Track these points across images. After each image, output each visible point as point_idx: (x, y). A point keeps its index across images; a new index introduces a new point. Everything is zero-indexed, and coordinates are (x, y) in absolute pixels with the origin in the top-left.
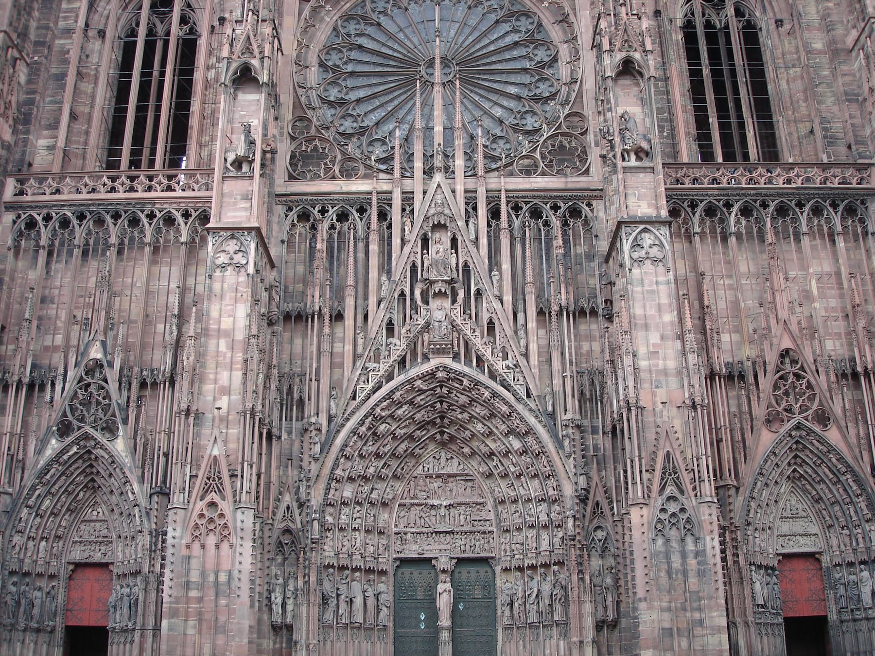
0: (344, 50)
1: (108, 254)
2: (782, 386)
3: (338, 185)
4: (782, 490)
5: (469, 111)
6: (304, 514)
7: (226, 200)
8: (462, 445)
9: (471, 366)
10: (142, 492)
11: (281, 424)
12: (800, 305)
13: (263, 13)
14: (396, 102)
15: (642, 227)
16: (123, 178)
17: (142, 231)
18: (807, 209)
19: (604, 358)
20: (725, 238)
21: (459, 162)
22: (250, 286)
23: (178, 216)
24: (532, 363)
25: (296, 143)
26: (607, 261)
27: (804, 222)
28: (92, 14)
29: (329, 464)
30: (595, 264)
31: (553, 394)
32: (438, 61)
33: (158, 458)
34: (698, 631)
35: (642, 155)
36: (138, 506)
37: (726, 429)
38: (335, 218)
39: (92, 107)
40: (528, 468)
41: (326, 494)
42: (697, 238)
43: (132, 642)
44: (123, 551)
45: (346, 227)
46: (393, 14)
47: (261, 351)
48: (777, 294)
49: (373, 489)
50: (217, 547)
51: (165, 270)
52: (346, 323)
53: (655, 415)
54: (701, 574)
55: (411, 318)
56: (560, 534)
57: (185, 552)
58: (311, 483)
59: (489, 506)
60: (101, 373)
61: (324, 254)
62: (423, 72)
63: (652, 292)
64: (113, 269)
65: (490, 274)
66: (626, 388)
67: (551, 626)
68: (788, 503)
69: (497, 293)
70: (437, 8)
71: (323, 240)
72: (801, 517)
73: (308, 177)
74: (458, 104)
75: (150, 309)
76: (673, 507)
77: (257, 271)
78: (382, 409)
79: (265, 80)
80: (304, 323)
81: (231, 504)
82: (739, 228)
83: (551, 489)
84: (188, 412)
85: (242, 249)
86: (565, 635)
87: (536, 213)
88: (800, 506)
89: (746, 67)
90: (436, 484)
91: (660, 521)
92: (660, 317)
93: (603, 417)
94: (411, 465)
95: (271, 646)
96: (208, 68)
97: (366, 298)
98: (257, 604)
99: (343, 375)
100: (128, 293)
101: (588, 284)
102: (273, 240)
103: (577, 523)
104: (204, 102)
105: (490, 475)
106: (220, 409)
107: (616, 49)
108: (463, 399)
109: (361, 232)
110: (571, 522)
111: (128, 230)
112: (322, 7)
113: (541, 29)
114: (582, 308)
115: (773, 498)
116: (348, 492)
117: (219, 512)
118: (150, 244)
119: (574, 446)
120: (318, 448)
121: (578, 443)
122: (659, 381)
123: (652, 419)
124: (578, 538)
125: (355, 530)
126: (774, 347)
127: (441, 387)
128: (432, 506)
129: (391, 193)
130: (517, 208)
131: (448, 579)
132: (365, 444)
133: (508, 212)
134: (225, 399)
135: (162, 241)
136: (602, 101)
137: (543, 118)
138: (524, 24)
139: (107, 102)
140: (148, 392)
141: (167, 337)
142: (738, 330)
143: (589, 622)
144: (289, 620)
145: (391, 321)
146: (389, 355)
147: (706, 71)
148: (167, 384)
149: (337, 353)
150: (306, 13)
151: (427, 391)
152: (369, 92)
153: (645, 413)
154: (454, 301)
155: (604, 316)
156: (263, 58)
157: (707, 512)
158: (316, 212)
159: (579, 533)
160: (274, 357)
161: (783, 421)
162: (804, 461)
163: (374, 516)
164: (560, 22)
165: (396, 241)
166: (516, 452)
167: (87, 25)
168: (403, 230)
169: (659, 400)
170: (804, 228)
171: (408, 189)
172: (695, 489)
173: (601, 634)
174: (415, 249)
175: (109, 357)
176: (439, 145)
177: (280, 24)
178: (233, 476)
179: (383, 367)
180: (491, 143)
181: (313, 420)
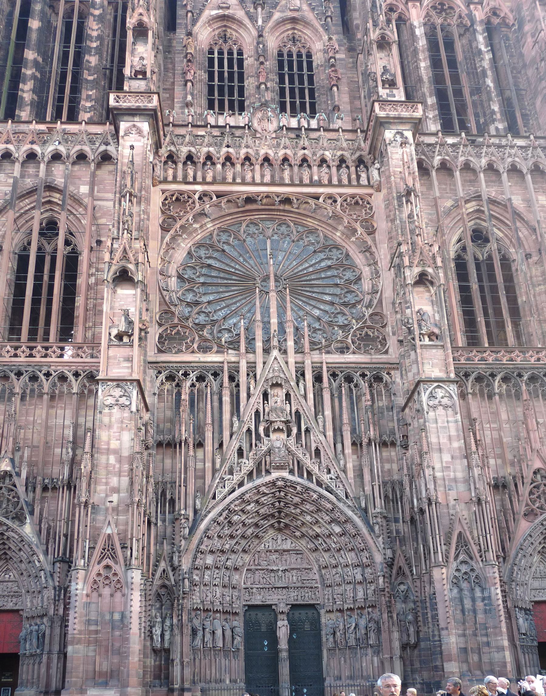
0: (197, 268)
1: (13, 399)
2: (536, 492)
6: (177, 575)
7: (110, 361)
11: (157, 516)
14: (238, 304)
16: (24, 348)
17: (41, 386)
24: (349, 476)
29: (195, 540)
31: (366, 497)
33: (60, 538)
36: (43, 570)
38: (195, 379)
43: (40, 663)
44: (32, 602)
51: (60, 412)
52: (206, 448)
55: (256, 445)
56: (373, 588)
60: (11, 480)
65: (316, 417)
69: (322, 430)
73: (174, 352)
75: (49, 439)
86: (378, 651)
87: (349, 379)
93: (403, 512)
96: (89, 276)
97: (221, 432)
98: (143, 635)
99: (204, 484)
100: (31, 427)
103: (386, 580)
108: (297, 500)
110: (381, 580)
116: (209, 560)
118: (47, 394)
120: (187, 531)
121: (385, 528)
124: (387, 590)
127: (280, 491)
129: (238, 363)
130: (334, 375)
132: (222, 529)
135: (57, 392)
140: (49, 494)
144: (166, 645)
145: (240, 448)
146: (241, 470)
147: (475, 286)
148: (65, 487)
149: (199, 469)
151: (268, 494)
152: (216, 296)
159: (388, 587)
164: (365, 251)
165: (243, 395)
168: (249, 388)
171: (252, 360)
173: (405, 652)
175: (17, 469)
176: (275, 331)
179: (236, 478)
181: (183, 512)
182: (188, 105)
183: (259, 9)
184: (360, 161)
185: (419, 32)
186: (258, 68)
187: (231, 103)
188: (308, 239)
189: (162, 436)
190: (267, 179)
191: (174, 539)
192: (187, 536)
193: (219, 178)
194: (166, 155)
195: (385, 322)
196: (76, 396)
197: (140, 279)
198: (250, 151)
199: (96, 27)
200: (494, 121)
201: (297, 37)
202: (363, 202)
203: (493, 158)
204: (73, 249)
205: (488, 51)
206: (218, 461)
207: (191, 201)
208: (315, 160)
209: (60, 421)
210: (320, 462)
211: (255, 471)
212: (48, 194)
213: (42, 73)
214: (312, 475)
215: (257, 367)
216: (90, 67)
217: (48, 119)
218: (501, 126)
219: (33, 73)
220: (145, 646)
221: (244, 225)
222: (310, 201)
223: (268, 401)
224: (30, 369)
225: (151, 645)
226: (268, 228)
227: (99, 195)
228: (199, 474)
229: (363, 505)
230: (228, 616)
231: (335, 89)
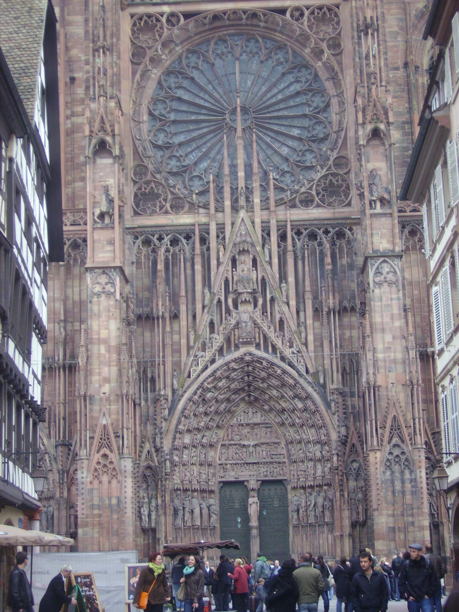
3: (170, 219)
6: (159, 456)
11: (140, 395)
13: (109, 90)
14: (209, 144)
15: (382, 259)
21: (257, 200)
25: (137, 186)
29: (174, 421)
30: (355, 273)
32: (239, 109)
34: (411, 529)
35: (384, 201)
38: (169, 243)
41: (173, 442)
45: (177, 250)
49: (203, 436)
50: (110, 482)
54: (413, 493)
55: (226, 319)
56: (329, 465)
57: (89, 486)
58: (163, 436)
59: (283, 444)
62: (228, 119)
63: (388, 306)
66: (368, 374)
67: (323, 525)
69: (285, 300)
70: (237, 63)
76: (397, 452)
78: (208, 383)
80: (151, 321)
85: (111, 281)
86: (332, 531)
87: (313, 236)
90: (246, 431)
91: (388, 460)
92: (393, 322)
95: (142, 542)
103: (340, 459)
105: (283, 424)
106: (104, 393)
107: (367, 121)
108: (263, 374)
109: (188, 255)
110: (335, 458)
112: (149, 70)
116: (187, 439)
117: (109, 460)
119: (338, 407)
120: (166, 412)
121: (340, 405)
123: (385, 393)
124: (340, 468)
125: (192, 464)
127: (248, 366)
129: (209, 225)
130: (299, 233)
131: (256, 495)
134: (107, 385)
137: (318, 156)
138: (304, 74)
143: (347, 523)
144: (153, 525)
150: (138, 76)
153: (381, 389)
154: (255, 306)
157: (418, 455)
163: (205, 454)
165: (214, 262)
166: (300, 410)
172: (411, 440)
174: (227, 268)
176: (242, 188)
177: (120, 90)
179: (208, 355)
181: (162, 393)
188: (277, 57)
189: (141, 309)
191: (155, 420)
192: (167, 417)
202: (331, 14)
206: (192, 337)
207: (159, 25)
210: (284, 336)
211: (225, 346)
214: (276, 349)
220: (136, 525)
221: (212, 43)
223: (236, 269)
225: (141, 525)
226: (237, 45)
228: (176, 347)
229: (322, 381)
230: (205, 495)
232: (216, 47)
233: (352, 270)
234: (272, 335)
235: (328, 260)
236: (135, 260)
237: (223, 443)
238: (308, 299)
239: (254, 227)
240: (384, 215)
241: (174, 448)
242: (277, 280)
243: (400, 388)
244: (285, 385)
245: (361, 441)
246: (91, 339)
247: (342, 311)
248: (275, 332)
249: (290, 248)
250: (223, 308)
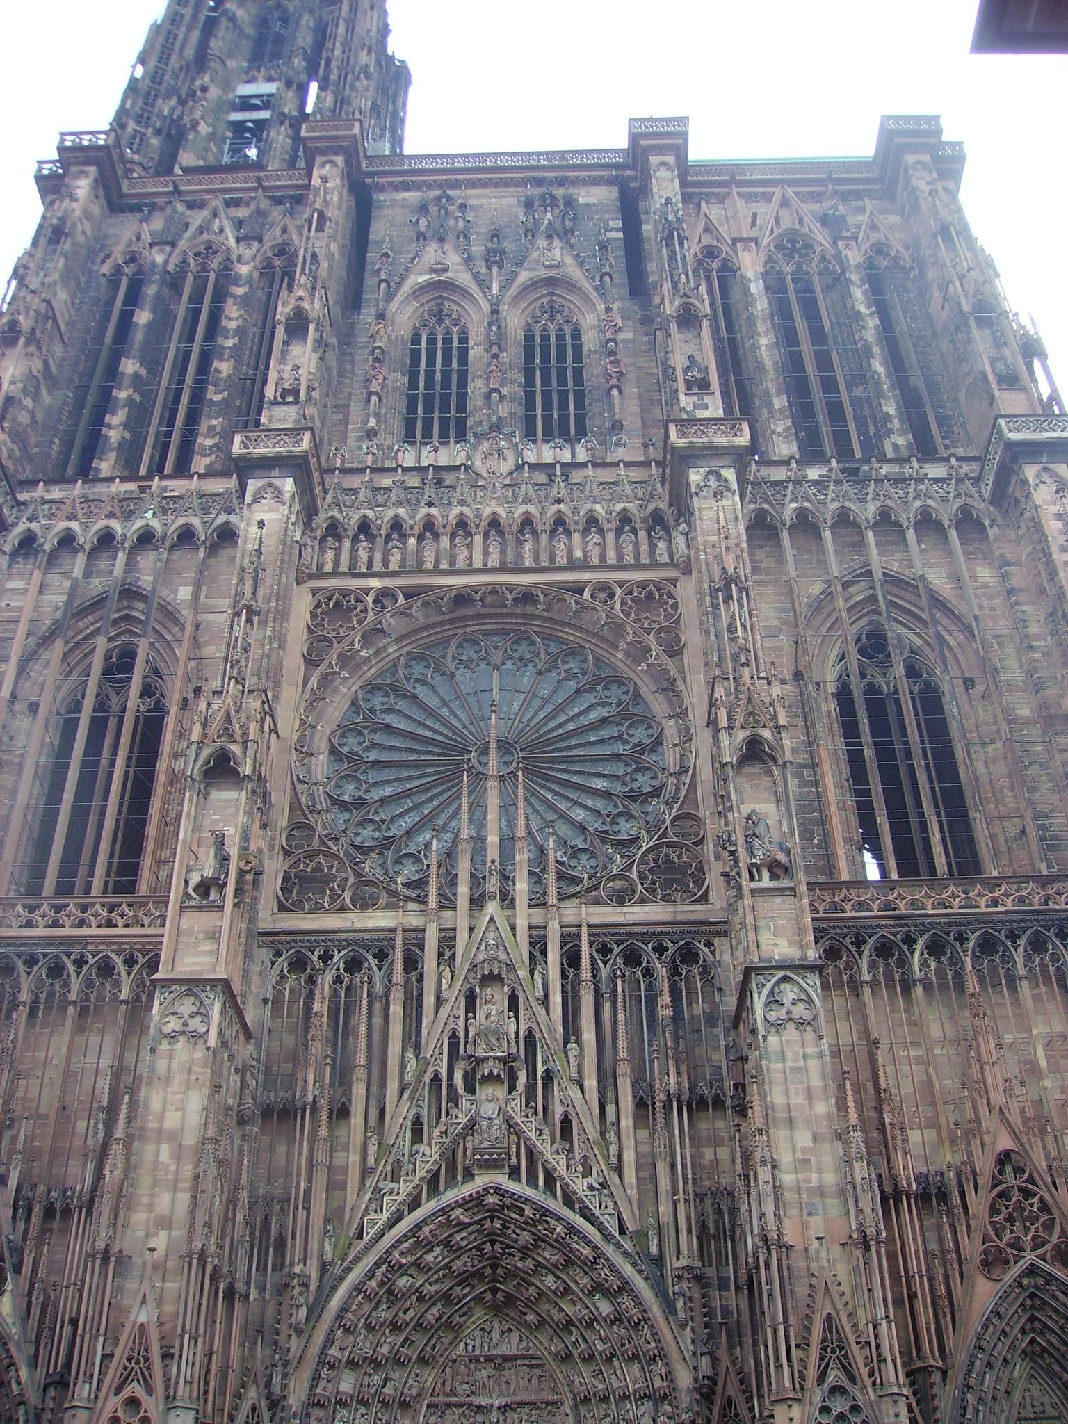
1: (14, 1016)
3: (348, 919)
4: (1016, 1373)
5: (539, 813)
8: (524, 1310)
9: (536, 1187)
10: (32, 1381)
11: (249, 1275)
12: (1022, 1083)
13: (251, 681)
14: (436, 803)
15: (780, 974)
17: (66, 984)
18: (1022, 942)
19: (735, 1171)
20: (907, 989)
21: (522, 886)
22: (210, 1065)
23: (118, 961)
24: (626, 1181)
26: (736, 1027)
27: (1020, 962)
28: (22, 681)
29: (319, 1338)
30: (719, 1031)
31: (659, 1228)
32: (493, 746)
33: (62, 1327)
35: (778, 871)
37: (921, 1277)
39: (12, 807)
40: (623, 1345)
41: (313, 1387)
42: (866, 989)
45: (358, 980)
46: (434, 682)
47: (220, 1163)
48: (986, 1068)
49: (386, 1380)
51: (94, 1040)
53: (807, 1258)
55: (448, 1114)
58: (290, 1370)
59: (567, 1408)
61: (325, 1020)
62: (474, 760)
64: (20, 1037)
66: (762, 1216)
68: (1027, 1394)
69: (575, 1075)
71: (323, 998)
72: (1051, 1418)
74: (521, 804)
76: (839, 1405)
77: (224, 1043)
78: (402, 1254)
79: (248, 772)
81: (161, 1401)
82: (926, 973)
83: (658, 1377)
84: (106, 1255)
85: (202, 1011)
87: (632, 958)
88: (1046, 1399)
89: (928, 746)
92: (811, 1108)
93: (735, 1263)
94: (446, 1341)
96: (176, 756)
97: (383, 1085)
99: (345, 1201)
101: (710, 1059)
102: (251, 998)
104: (165, 802)
105: (567, 1358)
106: (153, 1250)
107: (737, 724)
108: (525, 1237)
109: (378, 988)
111: (47, 981)
112: (336, 673)
113: (639, 700)
114: (702, 1096)
115: (1002, 1387)
117: (142, 1414)
118: (75, 1003)
119: (691, 1309)
120: (303, 1312)
121: (697, 1305)
122: (813, 1204)
123: (802, 1264)
126: (986, 1148)
127: (492, 1219)
128: (479, 1407)
129: (424, 930)
130: (604, 951)
133: (592, 956)
134: (163, 1234)
135: (93, 998)
136: (722, 797)
137: (643, 824)
138: (615, 694)
139: (33, 801)
140: (57, 1223)
141: (90, 1142)
142: (933, 1124)
145: (418, 1118)
146: (414, 1170)
147: (869, 752)
150: (314, 681)
151: (467, 1225)
153: (793, 1255)
154: (512, 1089)
155: (733, 1107)
156: (247, 742)
157: (892, 1412)
158: (315, 958)
160: (244, 1173)
161: (1007, 1262)
162: (1045, 1325)
164: (664, 690)
165: (429, 1000)
167: (14, 695)
168: (439, 984)
169: (813, 1234)
170: (1021, 970)
172: (871, 1374)
174: (455, 1012)
176: (493, 861)
177: (276, 697)
178: (166, 1356)
179: (405, 1188)
180: (569, 859)
181: (297, 1270)
182: (371, 434)
183: (495, 269)
184: (656, 520)
185: (756, 288)
186: (489, 364)
187: (444, 424)
190: (494, 561)
193: (411, 562)
194: (325, 526)
195: (702, 832)
196: (124, 1006)
197: (248, 772)
198: (466, 510)
199: (235, 314)
200: (889, 432)
201: (556, 306)
203: (889, 502)
204: (157, 703)
205: (871, 314)
206: (372, 1149)
207: (360, 606)
208: (576, 522)
209: (91, 1060)
210: (570, 1150)
211: (443, 1170)
212: (125, 603)
213: (142, 393)
215: (458, 939)
216: (219, 379)
217: (143, 472)
218: (901, 441)
219: (129, 397)
222: (567, 597)
224: (53, 951)
226: (496, 648)
227: (210, 602)
229: (654, 1250)
231: (615, 392)
232: (460, 650)
233: (715, 1026)
234: (545, 1149)
235: (666, 998)
236: (270, 996)
237: (433, 1399)
238: (625, 1074)
239: (514, 935)
240: (780, 891)
241: (314, 1402)
242: (560, 1037)
243: (836, 1251)
244: (574, 1263)
245: (747, 1391)
246: (142, 1129)
247: (698, 1105)
248: (553, 1142)
249: (586, 973)
250: (444, 1092)
